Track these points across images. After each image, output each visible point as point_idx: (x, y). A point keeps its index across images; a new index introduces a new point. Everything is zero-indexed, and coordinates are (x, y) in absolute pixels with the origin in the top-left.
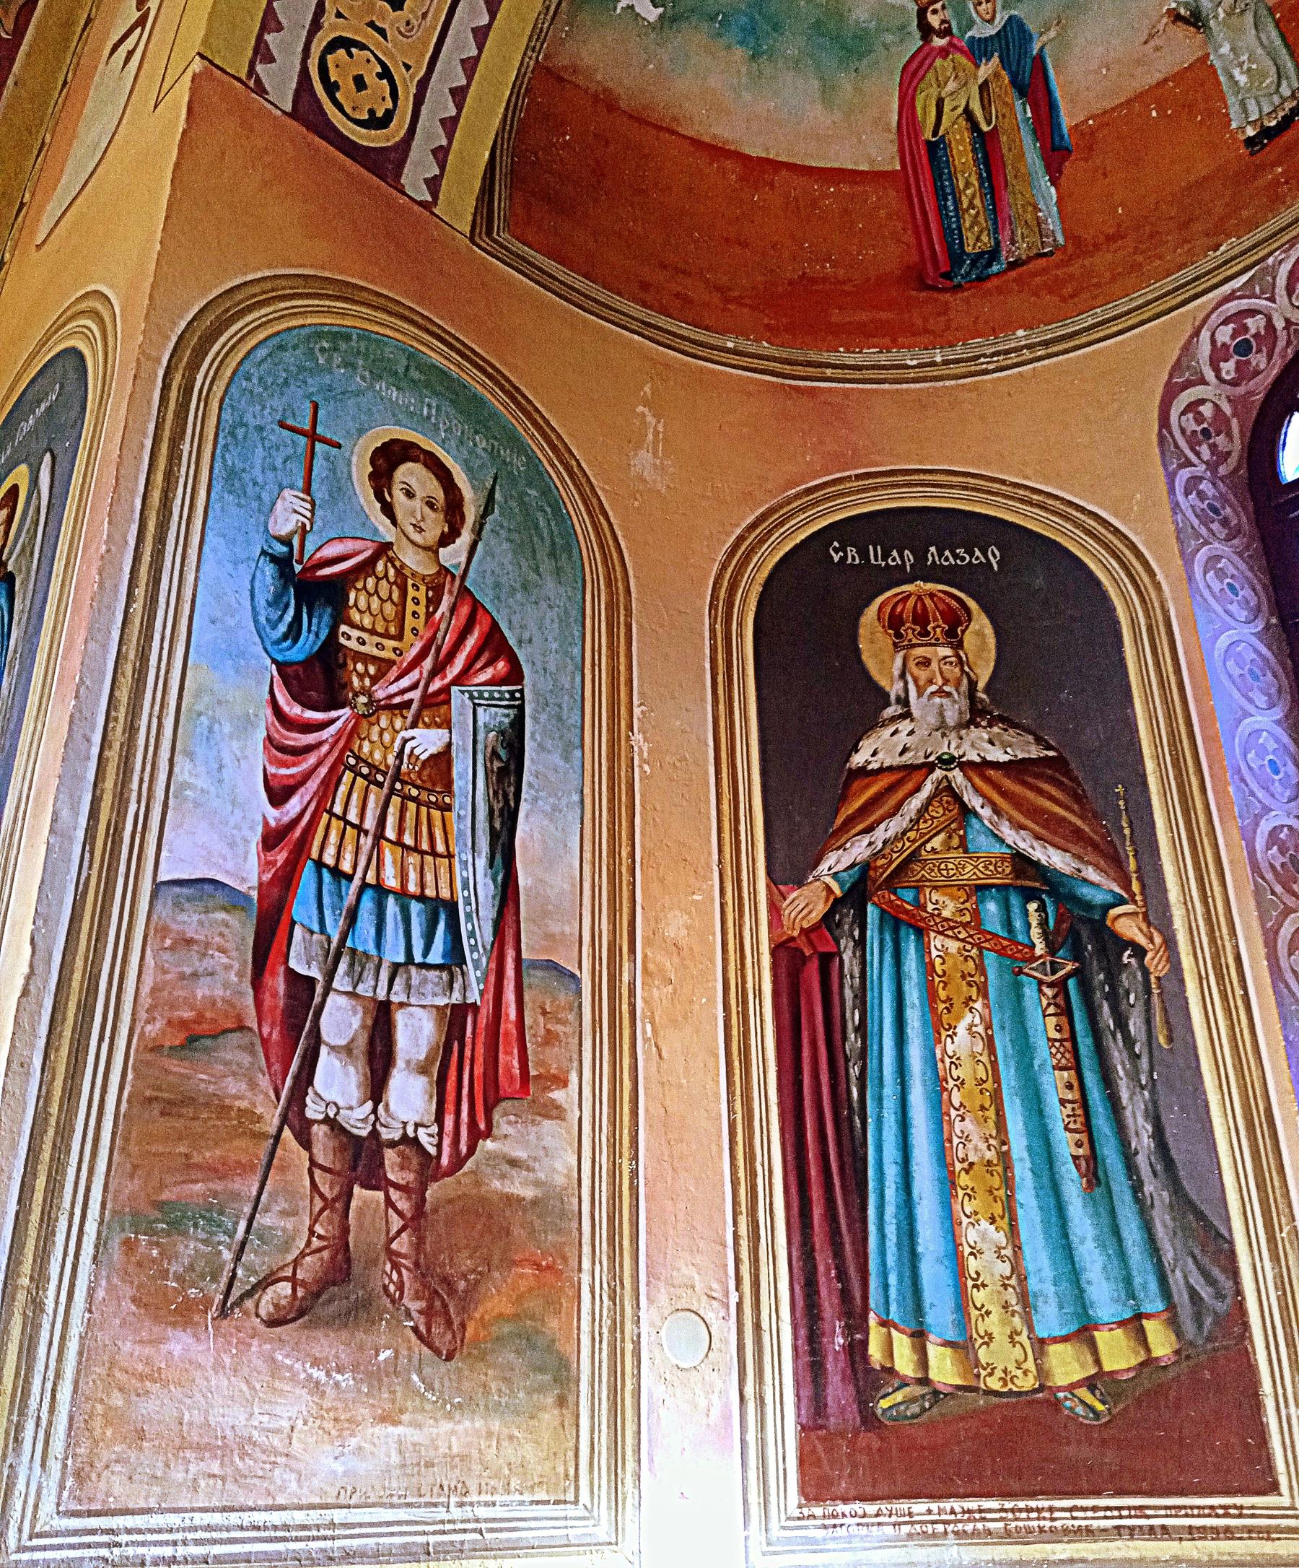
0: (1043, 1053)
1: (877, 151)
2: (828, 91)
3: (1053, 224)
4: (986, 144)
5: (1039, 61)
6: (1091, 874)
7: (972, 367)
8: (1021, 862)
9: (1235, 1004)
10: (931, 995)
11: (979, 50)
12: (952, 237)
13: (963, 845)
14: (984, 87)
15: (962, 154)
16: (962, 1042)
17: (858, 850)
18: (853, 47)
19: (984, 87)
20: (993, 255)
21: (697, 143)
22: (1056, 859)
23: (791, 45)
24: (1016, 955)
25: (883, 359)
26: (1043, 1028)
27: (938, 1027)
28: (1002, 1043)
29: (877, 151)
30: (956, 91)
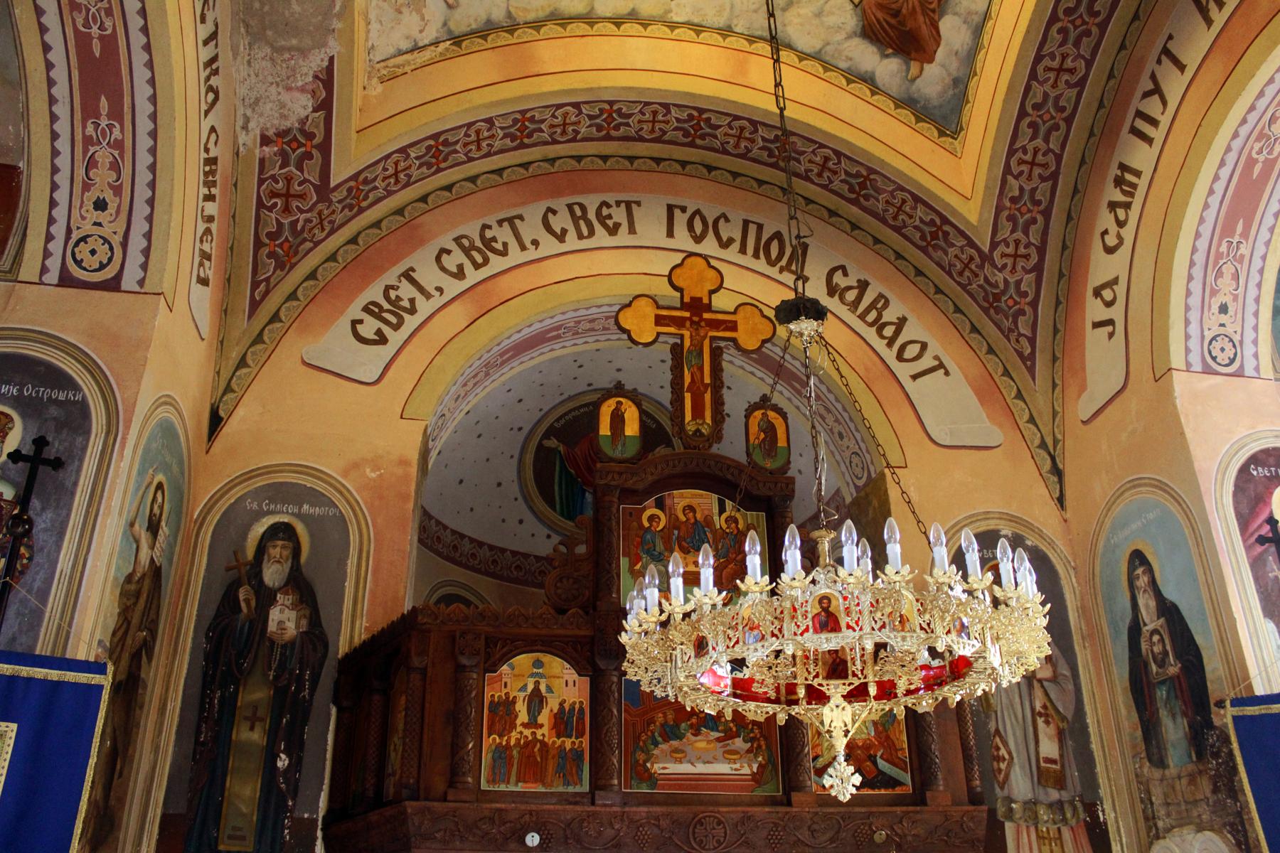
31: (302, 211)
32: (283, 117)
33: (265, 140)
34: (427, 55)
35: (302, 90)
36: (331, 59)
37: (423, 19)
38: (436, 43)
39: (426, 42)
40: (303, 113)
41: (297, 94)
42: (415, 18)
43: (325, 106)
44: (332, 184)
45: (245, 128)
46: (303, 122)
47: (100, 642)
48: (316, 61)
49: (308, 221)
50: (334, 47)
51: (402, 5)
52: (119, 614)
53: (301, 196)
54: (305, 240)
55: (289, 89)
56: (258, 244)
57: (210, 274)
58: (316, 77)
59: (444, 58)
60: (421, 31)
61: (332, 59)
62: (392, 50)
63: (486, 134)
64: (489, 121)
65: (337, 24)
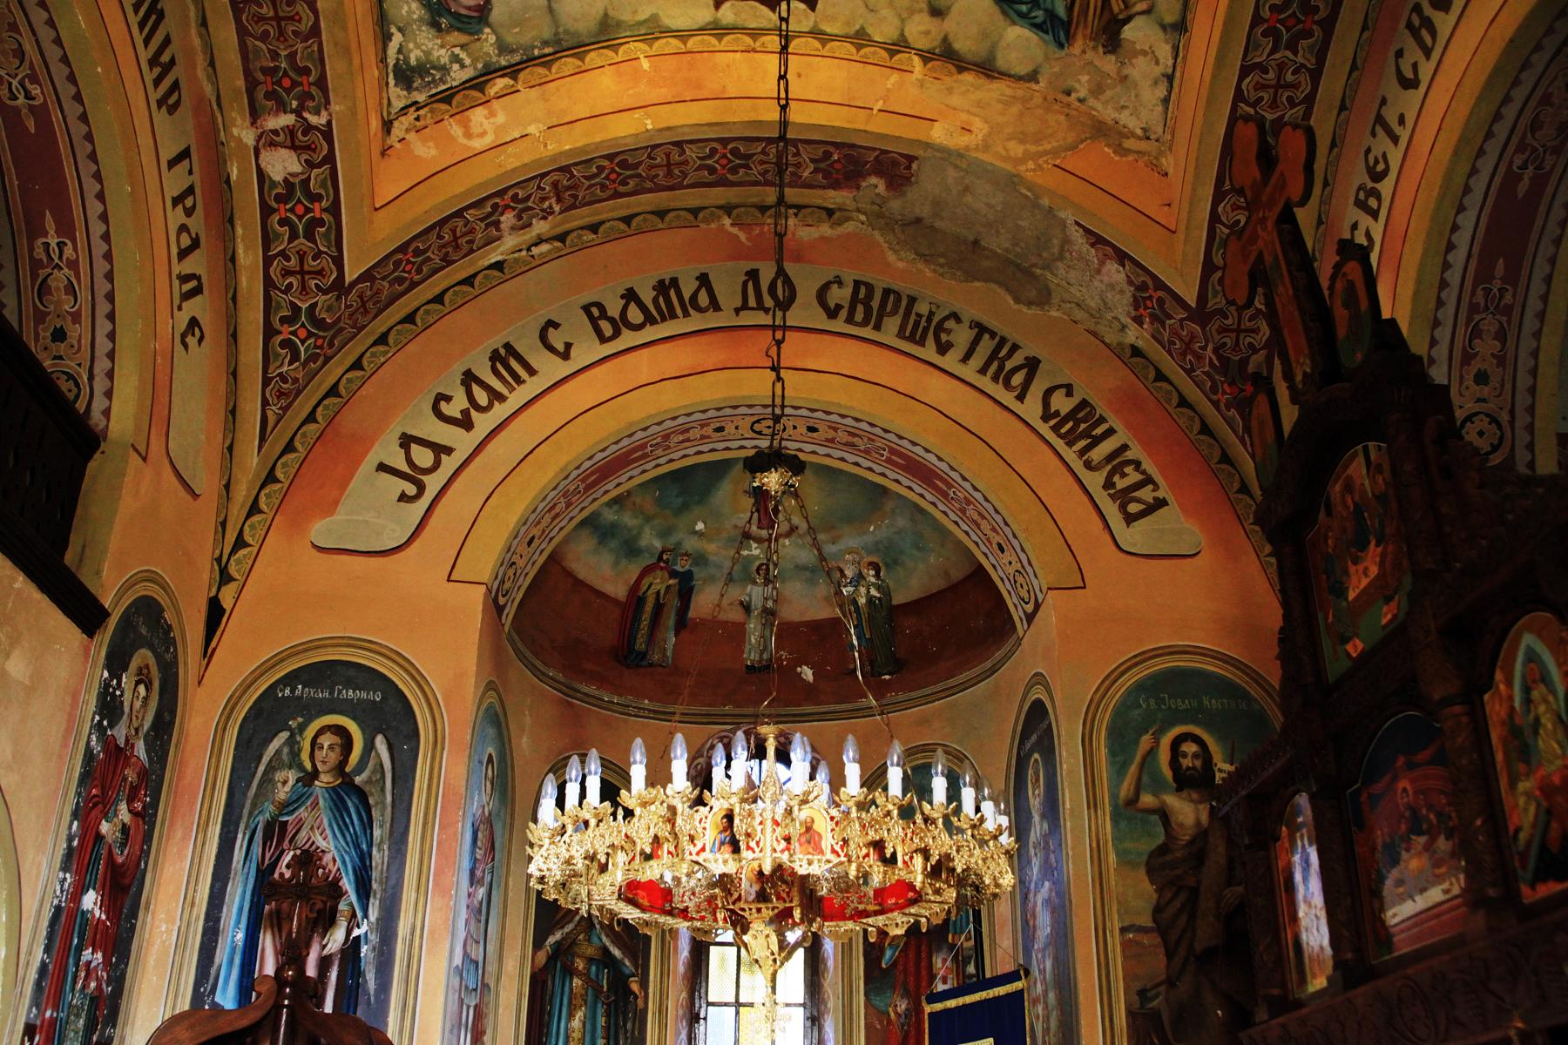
0: (599, 1031)
1: (619, 590)
2: (616, 563)
3: (669, 653)
4: (659, 608)
5: (691, 589)
6: (627, 962)
7: (624, 710)
8: (605, 950)
9: (663, 1026)
10: (570, 1003)
11: (674, 574)
12: (632, 638)
13: (589, 940)
14: (668, 587)
15: (649, 607)
16: (576, 1023)
17: (558, 936)
18: (631, 549)
19: (668, 587)
20: (643, 655)
21: (563, 568)
22: (617, 952)
23: (614, 544)
24: (597, 989)
25: (597, 693)
26: (601, 1021)
27: (571, 1016)
28: (588, 1027)
29: (619, 590)
30: (659, 583)
31: (1204, 348)
32: (1122, 292)
33: (1138, 321)
34: (1178, 74)
35: (1102, 263)
36: (1077, 223)
37: (1144, 53)
38: (1176, 50)
39: (1170, 62)
40: (1123, 275)
41: (1104, 270)
42: (1141, 62)
43: (1122, 257)
44: (1192, 301)
45: (1124, 327)
46: (1130, 282)
47: (1123, 930)
48: (1077, 236)
49: (1215, 351)
50: (1068, 215)
51: (1119, 72)
52: (1160, 891)
53: (1193, 337)
54: (1244, 362)
55: (1099, 272)
56: (1216, 404)
57: (1160, 494)
58: (1092, 245)
59: (1185, 58)
60: (1157, 63)
61: (1077, 223)
62: (1160, 108)
63: (1271, 75)
64: (1245, 71)
65: (1045, 202)
